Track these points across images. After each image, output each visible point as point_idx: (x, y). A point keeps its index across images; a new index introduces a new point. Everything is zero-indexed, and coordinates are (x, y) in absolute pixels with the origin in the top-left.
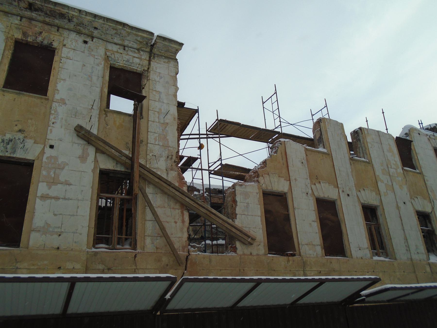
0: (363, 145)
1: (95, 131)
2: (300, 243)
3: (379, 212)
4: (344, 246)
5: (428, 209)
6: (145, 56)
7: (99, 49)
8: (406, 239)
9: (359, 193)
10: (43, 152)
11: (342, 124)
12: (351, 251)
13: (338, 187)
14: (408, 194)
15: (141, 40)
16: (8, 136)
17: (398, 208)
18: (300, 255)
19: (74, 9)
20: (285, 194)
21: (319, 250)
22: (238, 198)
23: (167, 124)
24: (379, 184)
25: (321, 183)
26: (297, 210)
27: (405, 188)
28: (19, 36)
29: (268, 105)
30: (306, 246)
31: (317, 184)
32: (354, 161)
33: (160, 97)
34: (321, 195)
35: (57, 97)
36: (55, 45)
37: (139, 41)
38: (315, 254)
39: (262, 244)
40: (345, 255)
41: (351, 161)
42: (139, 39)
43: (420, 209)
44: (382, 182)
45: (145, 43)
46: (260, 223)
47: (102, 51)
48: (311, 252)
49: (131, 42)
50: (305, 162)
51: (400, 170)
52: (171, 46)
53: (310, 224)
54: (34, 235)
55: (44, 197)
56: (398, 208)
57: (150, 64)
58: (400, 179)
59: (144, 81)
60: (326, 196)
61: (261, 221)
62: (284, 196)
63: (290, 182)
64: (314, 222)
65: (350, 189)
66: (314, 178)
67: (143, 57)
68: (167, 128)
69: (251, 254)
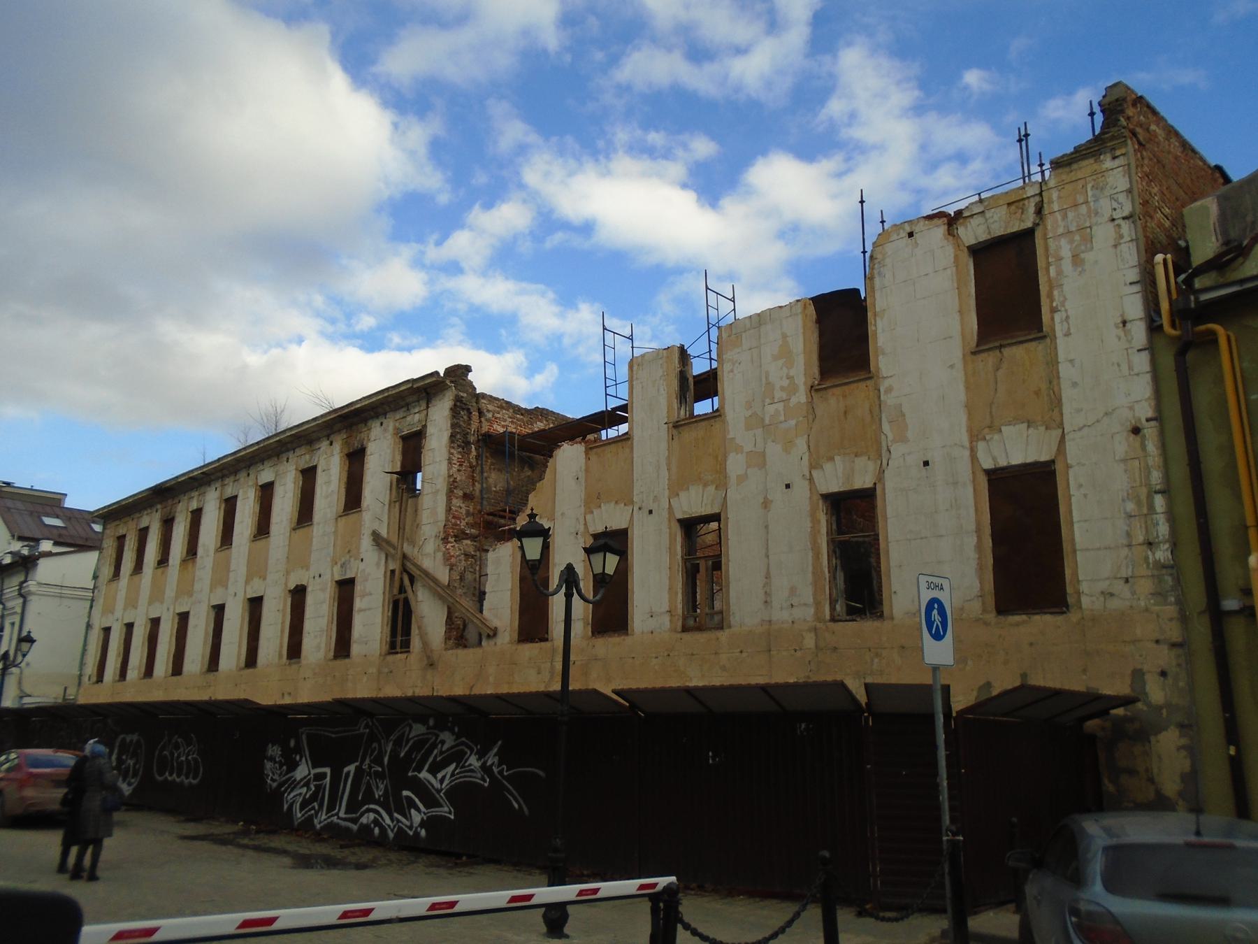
1: (384, 533)
6: (424, 405)
7: (391, 423)
13: (632, 502)
14: (806, 458)
17: (766, 504)
19: (357, 402)
31: (595, 512)
43: (835, 487)
44: (739, 449)
50: (582, 475)
55: (360, 610)
58: (793, 423)
65: (656, 499)
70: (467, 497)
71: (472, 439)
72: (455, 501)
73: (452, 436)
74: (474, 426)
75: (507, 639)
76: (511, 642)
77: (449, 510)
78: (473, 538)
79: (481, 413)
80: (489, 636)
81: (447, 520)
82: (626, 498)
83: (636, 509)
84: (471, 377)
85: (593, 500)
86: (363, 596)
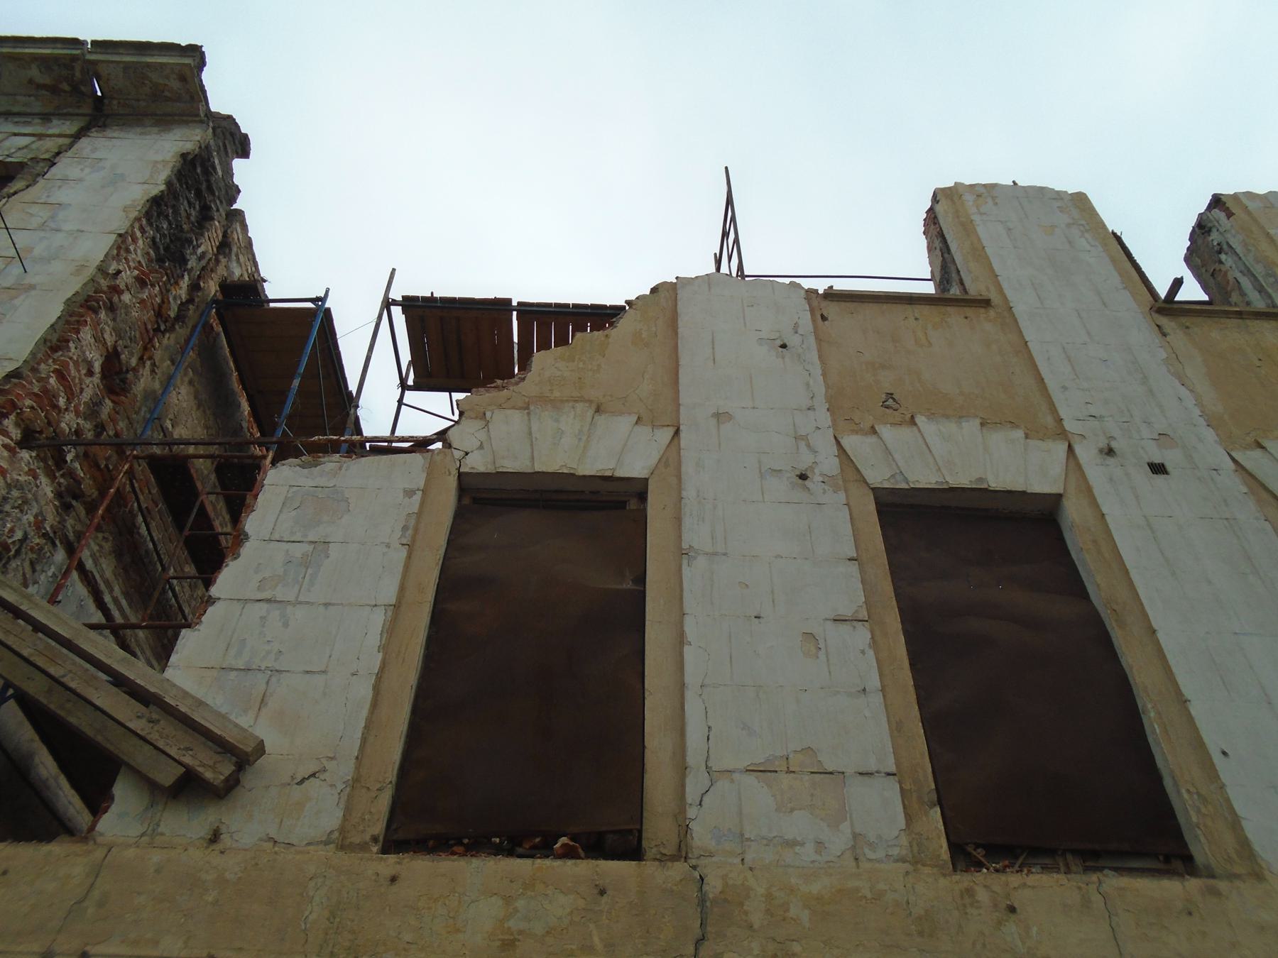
0: (1249, 260)
2: (694, 756)
4: (1168, 783)
9: (1258, 453)
11: (1080, 202)
12: (1235, 824)
15: (47, 80)
18: (681, 852)
20: (638, 490)
23: (32, 287)
25: (920, 420)
26: (701, 563)
30: (750, 779)
31: (886, 431)
32: (1183, 320)
33: (53, 217)
34: (923, 477)
37: (44, 87)
38: (839, 842)
39: (346, 769)
40: (1188, 859)
41: (1164, 321)
42: (34, 72)
45: (66, 87)
46: (374, 639)
48: (799, 825)
49: (19, 98)
52: (148, 65)
53: (809, 636)
57: (71, 146)
59: (18, 185)
60: (962, 479)
61: (390, 630)
62: (633, 505)
63: (677, 432)
64: (844, 628)
67: (50, 132)
68: (17, 302)
69: (215, 837)
70: (115, 375)
71: (192, 263)
72: (86, 334)
73: (156, 202)
74: (207, 245)
75: (323, 812)
76: (342, 842)
77: (56, 342)
78: (67, 497)
79: (224, 246)
80: (189, 789)
81: (32, 363)
83: (1086, 453)
84: (238, 164)
85: (865, 400)
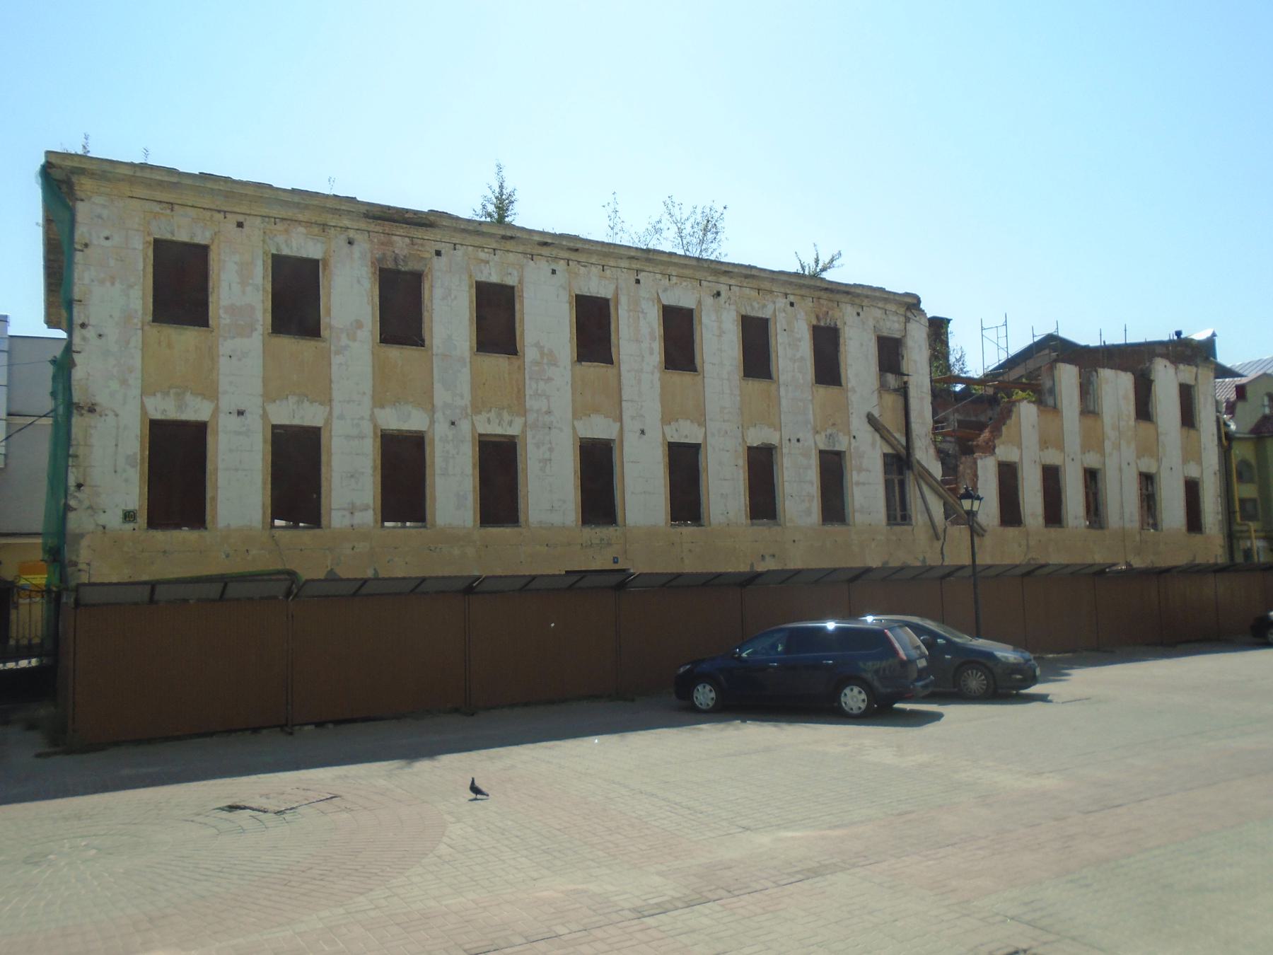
3: (1099, 476)
5: (1153, 470)
8: (1122, 506)
10: (850, 444)
16: (829, 431)
17: (1121, 470)
21: (1041, 520)
22: (980, 473)
24: (1107, 443)
27: (1133, 445)
28: (814, 322)
29: (990, 334)
35: (850, 385)
36: (839, 325)
43: (1144, 469)
47: (871, 323)
51: (1132, 422)
54: (857, 515)
55: (858, 484)
56: (1121, 470)
66: (1044, 444)
82: (1060, 446)
86: (860, 470)
